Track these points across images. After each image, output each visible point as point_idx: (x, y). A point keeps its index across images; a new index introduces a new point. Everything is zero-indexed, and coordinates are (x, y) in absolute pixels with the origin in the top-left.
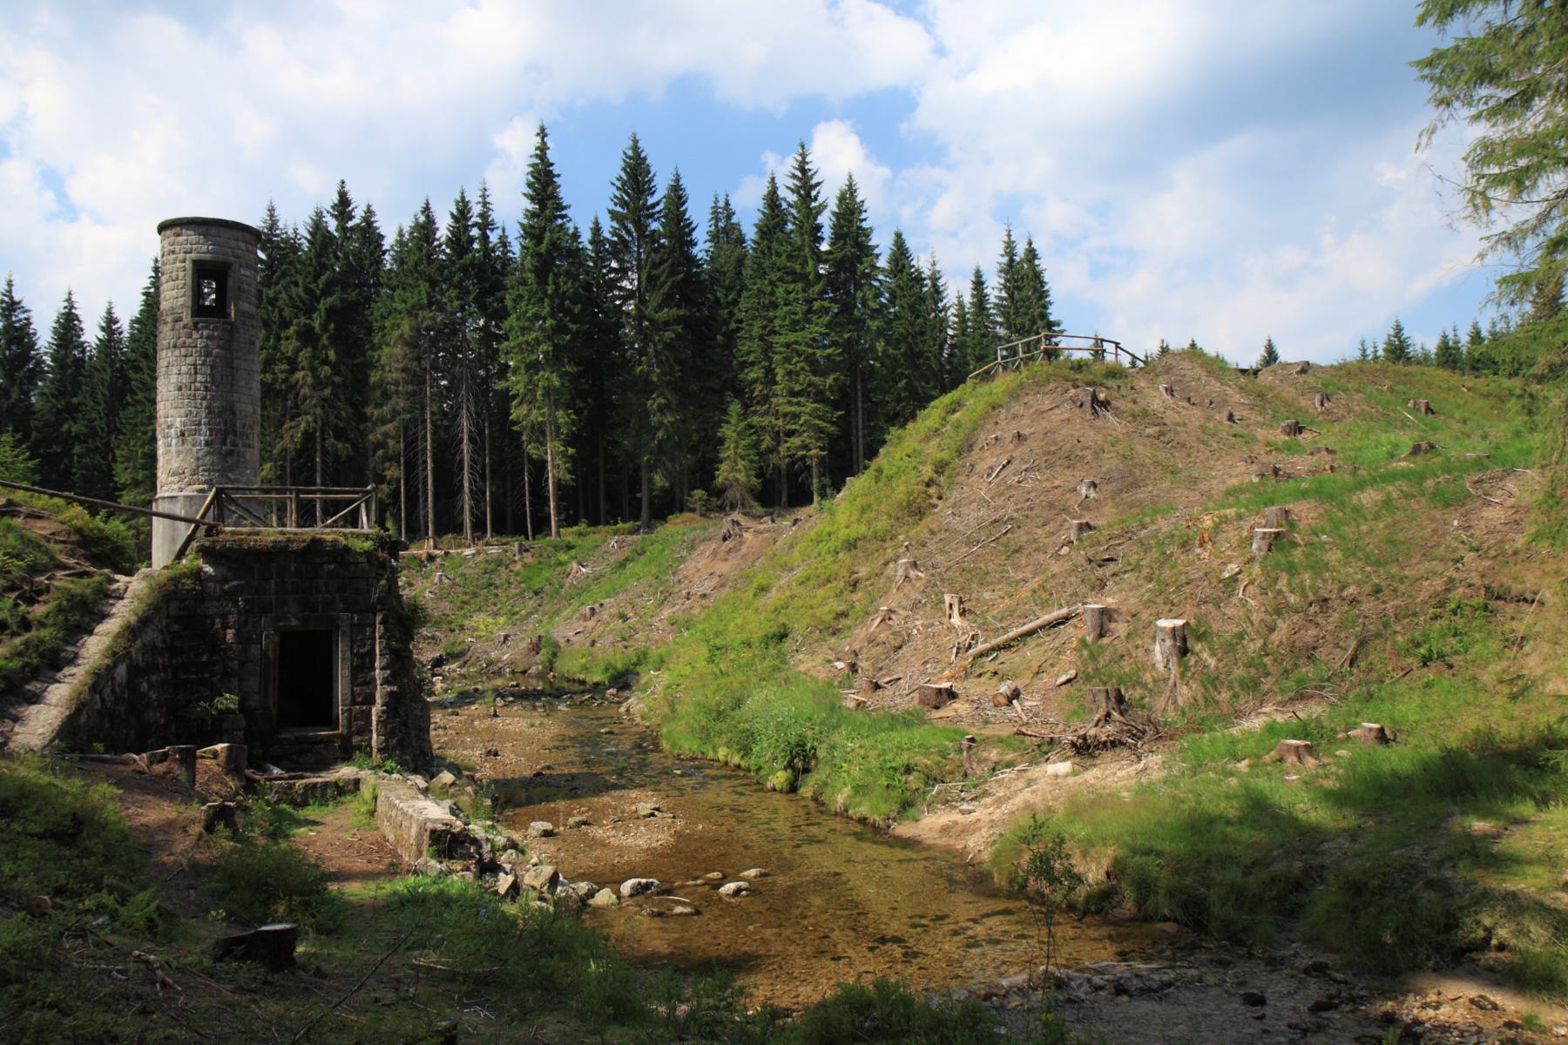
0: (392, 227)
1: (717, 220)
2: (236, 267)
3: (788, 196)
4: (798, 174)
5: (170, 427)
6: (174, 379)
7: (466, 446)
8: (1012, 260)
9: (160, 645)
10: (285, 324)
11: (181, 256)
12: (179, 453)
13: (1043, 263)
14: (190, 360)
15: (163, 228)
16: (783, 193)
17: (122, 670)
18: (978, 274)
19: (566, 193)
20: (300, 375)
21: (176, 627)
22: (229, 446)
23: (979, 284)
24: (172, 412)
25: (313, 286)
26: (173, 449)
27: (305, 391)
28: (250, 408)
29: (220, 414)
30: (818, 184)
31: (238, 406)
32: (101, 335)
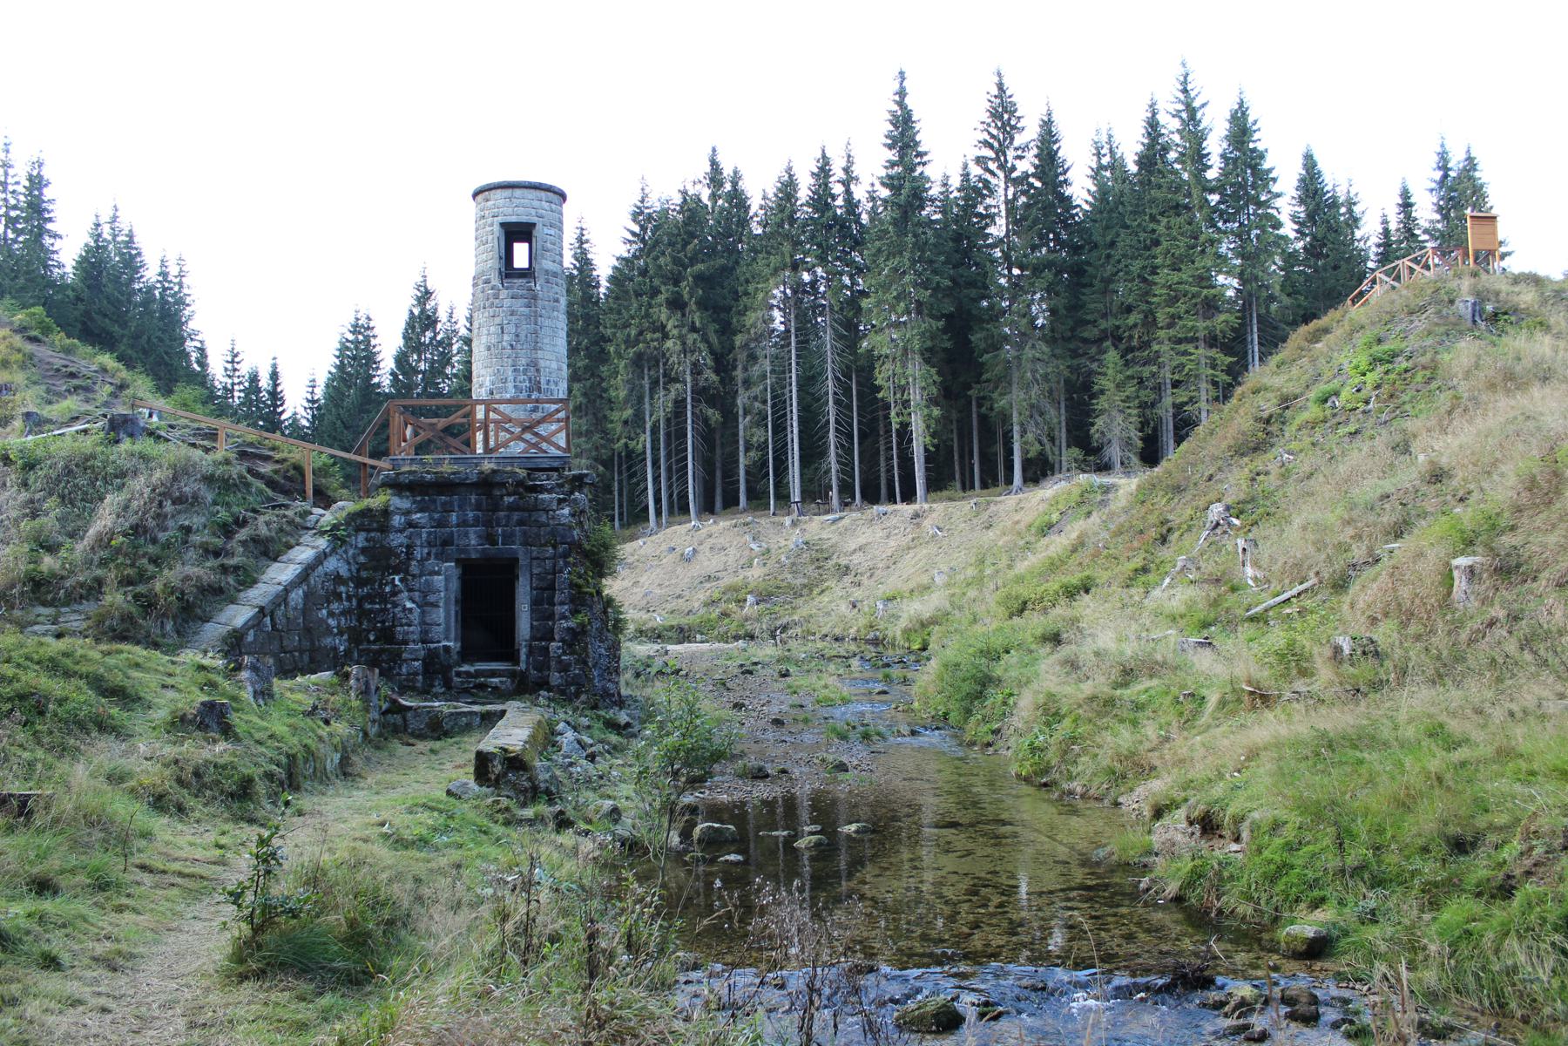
0: (759, 189)
1: (1098, 155)
2: (539, 227)
3: (1170, 125)
4: (1182, 97)
5: (481, 386)
6: (484, 339)
7: (831, 407)
8: (1446, 176)
9: (344, 572)
10: (655, 292)
13: (1483, 175)
14: (498, 320)
15: (475, 195)
16: (1163, 118)
17: (297, 596)
18: (1405, 194)
19: (926, 138)
20: (669, 344)
21: (362, 559)
23: (1406, 205)
24: (483, 372)
25: (681, 255)
27: (674, 359)
28: (554, 365)
30: (1203, 105)
31: (542, 363)
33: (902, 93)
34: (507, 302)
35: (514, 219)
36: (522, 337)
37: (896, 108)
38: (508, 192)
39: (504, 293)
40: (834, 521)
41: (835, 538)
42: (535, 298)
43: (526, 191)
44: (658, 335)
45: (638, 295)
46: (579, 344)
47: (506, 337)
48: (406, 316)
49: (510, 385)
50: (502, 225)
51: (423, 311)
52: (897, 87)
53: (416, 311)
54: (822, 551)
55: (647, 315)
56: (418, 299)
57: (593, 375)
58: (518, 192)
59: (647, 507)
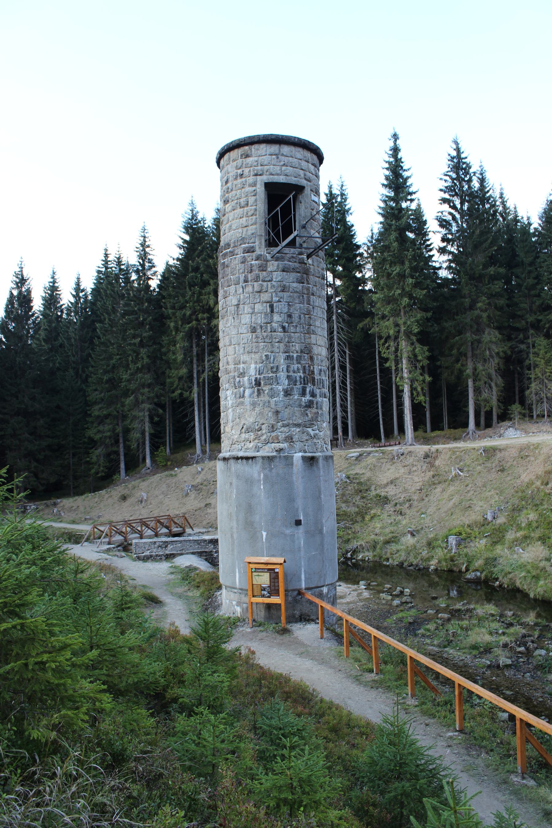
5: (242, 375)
6: (246, 319)
11: (251, 179)
12: (254, 405)
14: (265, 297)
15: (222, 154)
22: (308, 397)
24: (245, 357)
26: (247, 400)
29: (299, 359)
32: (73, 300)
33: (396, 150)
34: (277, 276)
35: (282, 179)
37: (392, 159)
38: (274, 148)
39: (272, 266)
40: (359, 458)
41: (368, 474)
42: (306, 272)
43: (292, 148)
44: (206, 315)
45: (191, 285)
46: (144, 320)
47: (276, 318)
48: (7, 295)
49: (282, 375)
51: (20, 293)
52: (392, 144)
53: (15, 293)
54: (360, 483)
55: (199, 301)
56: (17, 283)
57: (154, 343)
58: (286, 149)
59: (194, 440)
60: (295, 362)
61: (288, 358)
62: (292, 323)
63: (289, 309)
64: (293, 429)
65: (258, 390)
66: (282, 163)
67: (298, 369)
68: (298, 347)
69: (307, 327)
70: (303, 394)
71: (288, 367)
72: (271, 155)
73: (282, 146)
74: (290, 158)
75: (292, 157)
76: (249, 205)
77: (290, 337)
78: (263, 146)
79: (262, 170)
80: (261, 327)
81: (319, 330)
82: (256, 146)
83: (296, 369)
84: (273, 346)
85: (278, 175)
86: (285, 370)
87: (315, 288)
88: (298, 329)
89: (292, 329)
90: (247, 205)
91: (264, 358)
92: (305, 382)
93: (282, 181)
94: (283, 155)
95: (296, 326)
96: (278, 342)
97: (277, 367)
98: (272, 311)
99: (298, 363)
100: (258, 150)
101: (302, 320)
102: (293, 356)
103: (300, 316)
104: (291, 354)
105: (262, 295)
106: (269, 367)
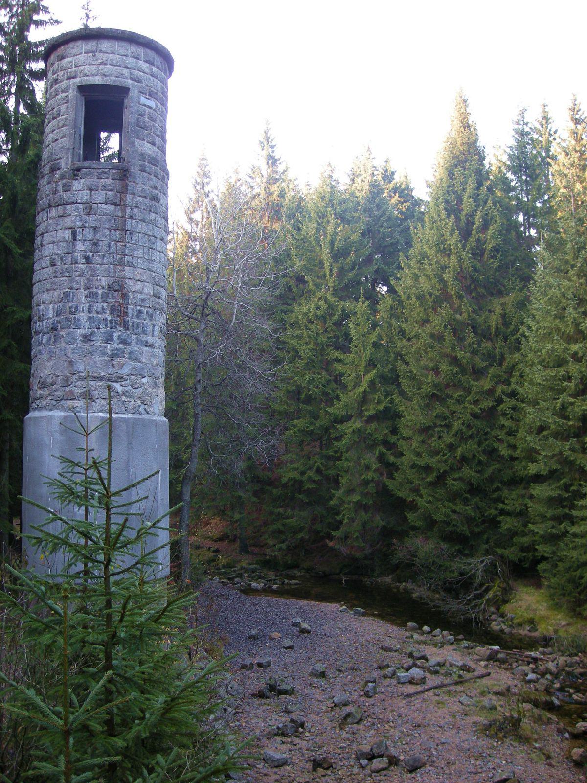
2: (134, 93)
14: (68, 221)
28: (149, 289)
35: (98, 80)
36: (103, 247)
47: (79, 246)
50: (83, 89)
58: (105, 45)
60: (100, 300)
61: (91, 295)
62: (98, 252)
63: (95, 235)
64: (92, 383)
65: (55, 336)
66: (100, 61)
67: (103, 308)
68: (104, 282)
69: (119, 257)
70: (109, 339)
71: (90, 307)
72: (86, 53)
73: (101, 41)
74: (111, 55)
75: (113, 53)
76: (61, 114)
77: (95, 270)
78: (79, 43)
79: (75, 72)
80: (62, 260)
81: (140, 261)
82: (71, 45)
83: (100, 309)
84: (72, 281)
85: (93, 75)
86: (86, 309)
87: (135, 210)
88: (106, 260)
89: (98, 260)
90: (59, 114)
91: (62, 295)
92: (113, 324)
93: (97, 83)
94: (101, 51)
95: (104, 256)
96: (79, 276)
97: (77, 307)
98: (74, 238)
99: (103, 302)
100: (73, 48)
101: (112, 249)
102: (97, 293)
103: (109, 244)
104: (95, 290)
105: (66, 219)
106: (68, 308)
